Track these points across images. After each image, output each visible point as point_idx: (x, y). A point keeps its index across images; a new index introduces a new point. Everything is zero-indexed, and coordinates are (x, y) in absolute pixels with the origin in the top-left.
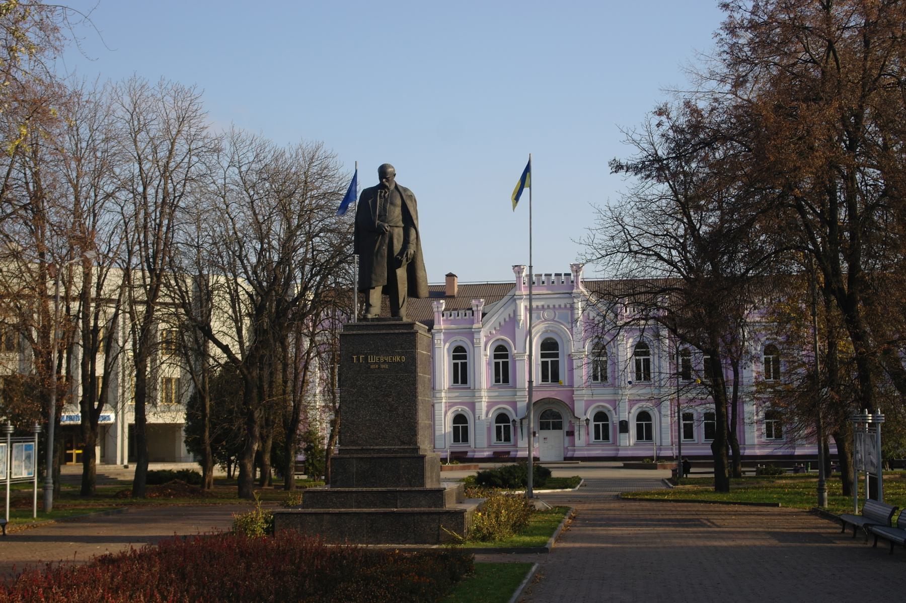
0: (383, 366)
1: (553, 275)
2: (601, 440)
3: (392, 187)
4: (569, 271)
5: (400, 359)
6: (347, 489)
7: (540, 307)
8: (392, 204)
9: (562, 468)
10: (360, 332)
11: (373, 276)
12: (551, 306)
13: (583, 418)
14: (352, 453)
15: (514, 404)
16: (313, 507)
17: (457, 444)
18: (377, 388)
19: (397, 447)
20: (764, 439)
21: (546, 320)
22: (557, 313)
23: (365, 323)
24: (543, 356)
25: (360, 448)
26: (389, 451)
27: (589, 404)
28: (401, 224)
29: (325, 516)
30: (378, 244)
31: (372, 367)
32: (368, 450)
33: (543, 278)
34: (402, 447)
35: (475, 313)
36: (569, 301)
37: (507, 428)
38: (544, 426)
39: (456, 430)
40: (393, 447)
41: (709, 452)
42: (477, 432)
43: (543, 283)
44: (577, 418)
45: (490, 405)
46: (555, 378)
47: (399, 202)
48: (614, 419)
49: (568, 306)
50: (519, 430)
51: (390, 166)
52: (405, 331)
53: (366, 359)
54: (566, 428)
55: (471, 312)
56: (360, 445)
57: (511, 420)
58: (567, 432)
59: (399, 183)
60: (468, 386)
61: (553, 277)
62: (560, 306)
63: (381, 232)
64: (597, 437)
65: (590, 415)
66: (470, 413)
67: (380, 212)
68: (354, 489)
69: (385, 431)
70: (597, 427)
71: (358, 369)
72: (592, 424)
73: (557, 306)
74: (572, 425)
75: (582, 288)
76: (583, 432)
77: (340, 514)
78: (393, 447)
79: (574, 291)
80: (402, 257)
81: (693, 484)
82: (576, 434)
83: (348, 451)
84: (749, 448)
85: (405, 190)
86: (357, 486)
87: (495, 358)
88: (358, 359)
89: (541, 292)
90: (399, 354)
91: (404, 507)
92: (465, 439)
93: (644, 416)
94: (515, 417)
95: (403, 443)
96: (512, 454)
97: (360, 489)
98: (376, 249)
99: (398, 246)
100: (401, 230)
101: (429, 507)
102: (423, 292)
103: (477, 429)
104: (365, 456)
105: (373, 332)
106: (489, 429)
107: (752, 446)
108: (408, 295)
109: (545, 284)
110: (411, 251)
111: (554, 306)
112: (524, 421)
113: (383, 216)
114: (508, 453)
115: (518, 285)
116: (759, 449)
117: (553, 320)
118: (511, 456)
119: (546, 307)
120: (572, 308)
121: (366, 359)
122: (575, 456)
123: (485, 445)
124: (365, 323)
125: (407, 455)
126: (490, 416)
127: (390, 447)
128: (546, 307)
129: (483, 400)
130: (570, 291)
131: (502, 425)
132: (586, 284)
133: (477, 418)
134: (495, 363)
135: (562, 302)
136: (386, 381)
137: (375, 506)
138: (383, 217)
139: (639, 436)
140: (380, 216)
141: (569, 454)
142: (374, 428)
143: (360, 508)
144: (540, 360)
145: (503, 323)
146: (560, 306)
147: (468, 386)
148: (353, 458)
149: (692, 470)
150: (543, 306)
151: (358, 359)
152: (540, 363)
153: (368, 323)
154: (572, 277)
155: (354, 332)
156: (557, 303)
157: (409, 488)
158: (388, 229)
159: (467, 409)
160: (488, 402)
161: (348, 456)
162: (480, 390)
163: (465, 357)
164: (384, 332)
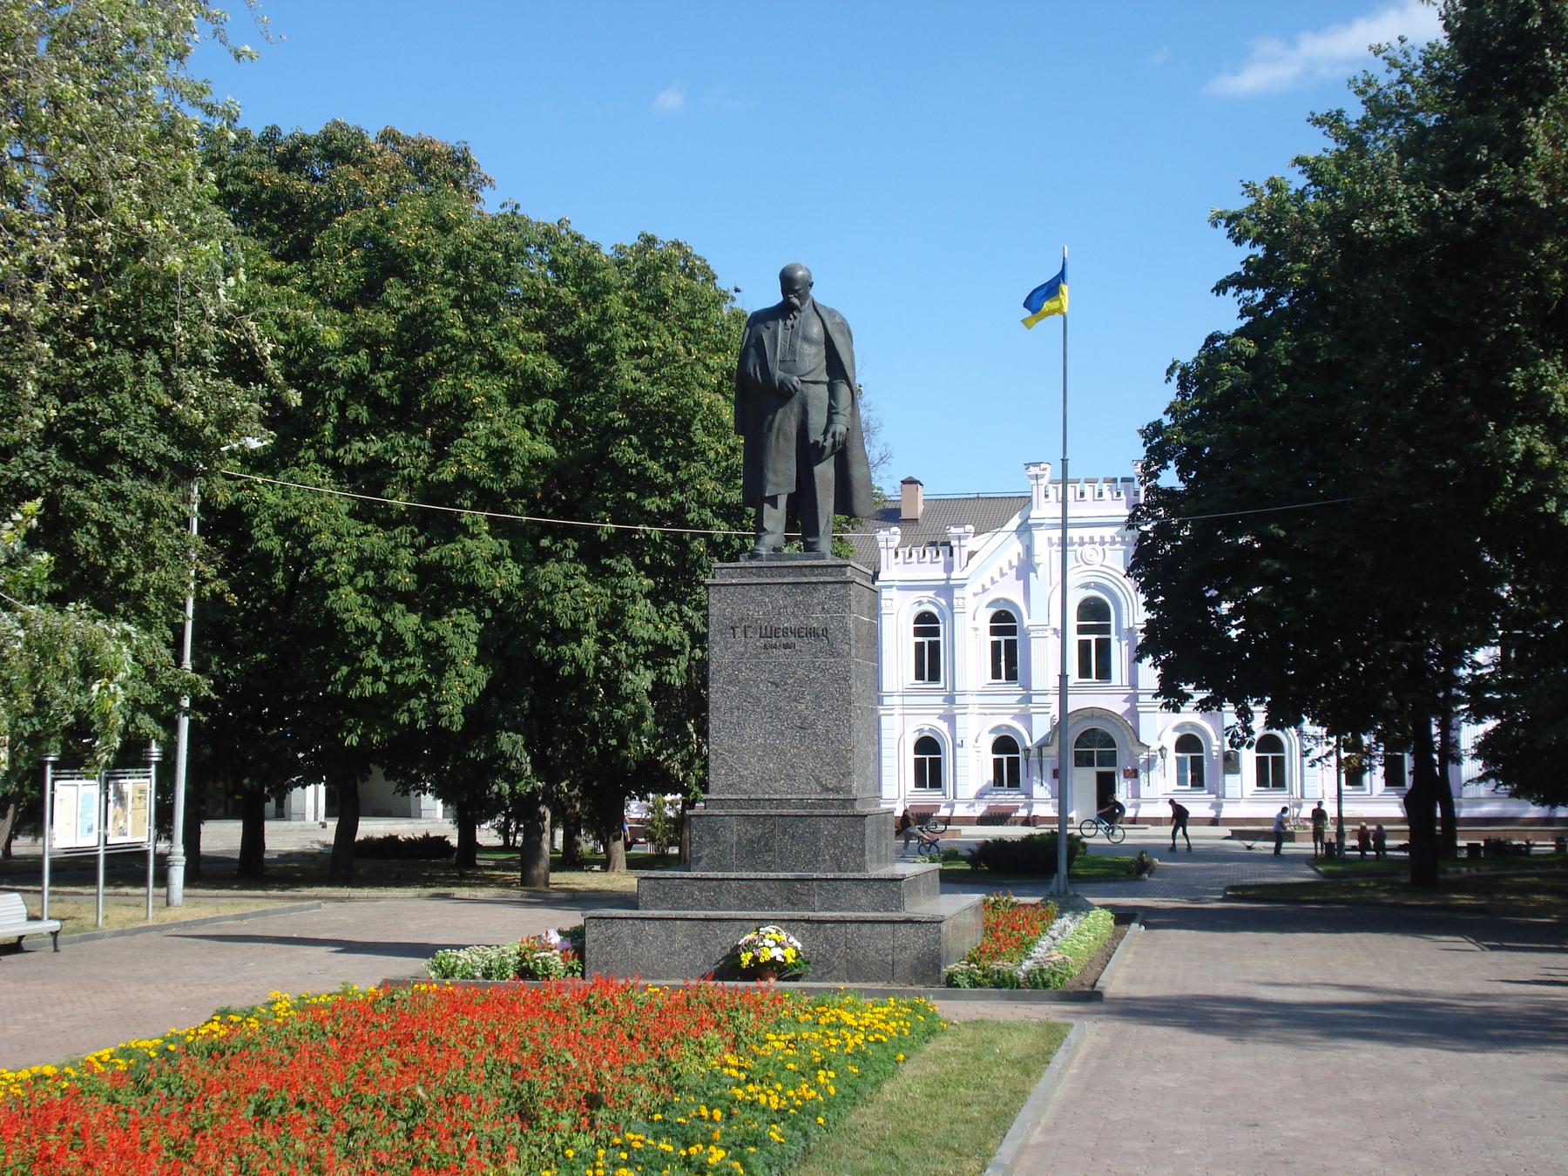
6: (720, 875)
12: (1097, 539)
13: (1155, 746)
14: (729, 807)
16: (656, 907)
22: (1107, 552)
23: (754, 563)
24: (1082, 630)
28: (826, 379)
29: (678, 922)
37: (1013, 764)
39: (919, 764)
46: (1104, 673)
52: (831, 579)
55: (948, 548)
59: (818, 300)
63: (784, 394)
65: (1170, 740)
67: (784, 355)
68: (733, 875)
69: (792, 767)
72: (1172, 755)
74: (1135, 757)
85: (832, 312)
86: (739, 869)
91: (826, 910)
92: (936, 782)
94: (1029, 744)
95: (828, 790)
97: (744, 875)
99: (817, 420)
101: (874, 910)
110: (840, 427)
112: (1045, 751)
113: (789, 364)
125: (833, 812)
131: (1005, 757)
137: (772, 905)
139: (1262, 781)
142: (771, 760)
143: (745, 909)
157: (838, 875)
158: (799, 386)
163: (936, 632)
164: (791, 580)
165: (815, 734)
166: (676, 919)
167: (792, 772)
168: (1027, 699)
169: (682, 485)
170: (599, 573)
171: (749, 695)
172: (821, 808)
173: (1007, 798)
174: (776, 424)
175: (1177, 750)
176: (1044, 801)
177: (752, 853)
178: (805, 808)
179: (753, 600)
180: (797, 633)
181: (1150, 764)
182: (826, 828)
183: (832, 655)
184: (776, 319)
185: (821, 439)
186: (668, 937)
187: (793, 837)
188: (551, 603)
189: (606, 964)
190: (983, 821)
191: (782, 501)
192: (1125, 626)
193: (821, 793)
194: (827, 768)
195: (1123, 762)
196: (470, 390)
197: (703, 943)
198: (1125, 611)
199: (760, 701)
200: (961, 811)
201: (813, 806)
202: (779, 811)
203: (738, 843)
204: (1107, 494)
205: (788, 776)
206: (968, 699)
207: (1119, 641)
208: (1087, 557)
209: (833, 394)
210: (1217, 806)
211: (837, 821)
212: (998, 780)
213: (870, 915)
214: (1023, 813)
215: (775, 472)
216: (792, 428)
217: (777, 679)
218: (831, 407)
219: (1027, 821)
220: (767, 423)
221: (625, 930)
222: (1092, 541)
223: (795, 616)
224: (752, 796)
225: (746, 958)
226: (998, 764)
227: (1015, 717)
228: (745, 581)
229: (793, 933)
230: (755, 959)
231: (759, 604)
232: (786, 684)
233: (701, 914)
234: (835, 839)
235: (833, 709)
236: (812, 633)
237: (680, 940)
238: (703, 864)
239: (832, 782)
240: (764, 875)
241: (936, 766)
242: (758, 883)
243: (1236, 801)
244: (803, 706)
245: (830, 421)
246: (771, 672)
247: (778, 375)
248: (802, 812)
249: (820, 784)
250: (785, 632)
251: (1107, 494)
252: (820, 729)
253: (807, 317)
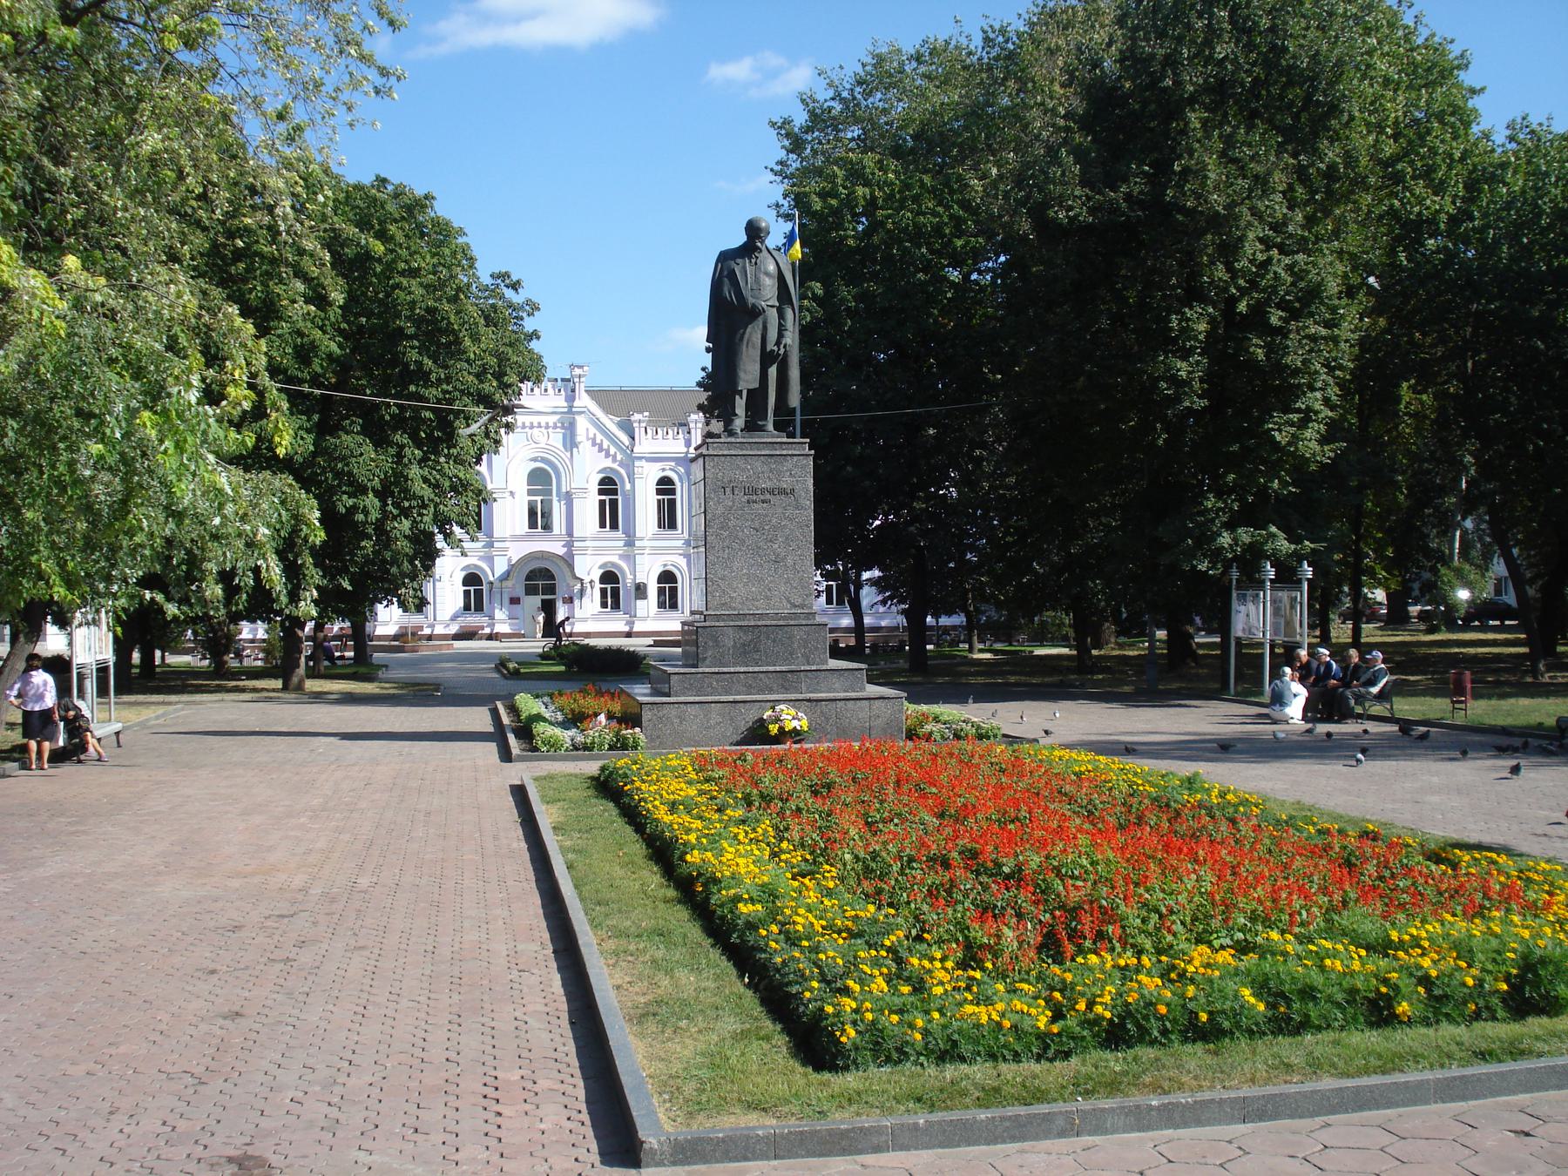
3: (764, 248)
6: (732, 670)
12: (543, 424)
13: (587, 580)
16: (684, 694)
24: (530, 493)
35: (693, 431)
37: (479, 594)
41: (902, 620)
46: (547, 527)
48: (627, 581)
55: (686, 428)
63: (755, 313)
64: (604, 605)
65: (596, 575)
70: (603, 592)
72: (598, 586)
74: (571, 588)
83: (718, 617)
93: (667, 577)
94: (491, 579)
97: (751, 669)
99: (773, 335)
137: (771, 691)
138: (756, 292)
139: (661, 605)
164: (767, 452)
168: (490, 545)
169: (448, 380)
170: (380, 442)
171: (736, 537)
173: (473, 620)
174: (746, 336)
175: (602, 582)
176: (503, 622)
177: (745, 653)
179: (738, 467)
180: (771, 492)
181: (582, 592)
182: (798, 634)
183: (797, 508)
184: (743, 257)
185: (776, 348)
186: (705, 716)
187: (774, 641)
188: (347, 465)
189: (658, 737)
190: (458, 637)
191: (745, 394)
192: (564, 490)
195: (561, 591)
196: (279, 295)
197: (731, 719)
198: (563, 479)
200: (439, 630)
201: (784, 618)
202: (764, 623)
203: (734, 646)
204: (550, 391)
205: (767, 597)
206: (646, 543)
207: (559, 501)
208: (536, 438)
209: (781, 316)
210: (630, 623)
211: (806, 628)
212: (467, 608)
213: (842, 695)
214: (487, 631)
216: (757, 339)
217: (757, 525)
218: (780, 325)
219: (490, 637)
220: (738, 336)
221: (673, 712)
222: (539, 426)
223: (770, 479)
225: (774, 729)
226: (467, 593)
227: (481, 558)
228: (745, 452)
229: (798, 709)
230: (781, 729)
231: (743, 470)
233: (731, 698)
234: (806, 641)
236: (783, 492)
237: (715, 718)
238: (707, 662)
239: (799, 601)
240: (764, 669)
242: (761, 675)
243: (644, 619)
245: (781, 335)
247: (751, 301)
248: (781, 623)
249: (789, 602)
250: (763, 491)
251: (550, 391)
252: (790, 561)
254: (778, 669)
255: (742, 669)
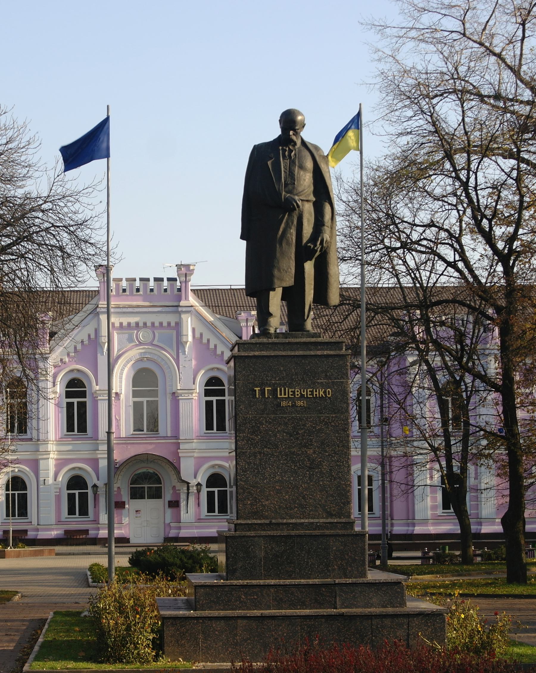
0: (300, 403)
1: (124, 280)
2: (217, 513)
3: (299, 143)
4: (175, 275)
5: (325, 392)
6: (262, 582)
7: (133, 325)
8: (302, 167)
9: (70, 554)
10: (264, 353)
11: (276, 272)
13: (193, 482)
14: (255, 530)
15: (94, 463)
16: (210, 609)
17: (11, 519)
18: (291, 436)
19: (322, 520)
20: (440, 511)
21: (141, 344)
22: (157, 335)
23: (265, 340)
24: (135, 394)
25: (267, 521)
26: (311, 526)
27: (200, 461)
29: (239, 621)
30: (283, 226)
31: (284, 404)
32: (278, 524)
33: (138, 283)
34: (329, 520)
36: (172, 319)
37: (84, 497)
38: (136, 494)
40: (316, 520)
42: (41, 502)
43: (124, 291)
44: (184, 481)
45: (60, 464)
47: (309, 164)
49: (173, 324)
50: (192, 499)
51: (300, 113)
52: (332, 353)
53: (274, 392)
54: (168, 496)
56: (266, 518)
57: (90, 486)
58: (169, 502)
59: (306, 139)
60: (28, 436)
61: (152, 283)
62: (161, 324)
64: (211, 509)
65: (202, 478)
66: (32, 475)
69: (304, 498)
70: (210, 495)
71: (262, 407)
72: (205, 491)
73: (157, 324)
75: (192, 300)
76: (192, 500)
77: (263, 618)
78: (316, 520)
79: (182, 303)
80: (315, 245)
81: (432, 573)
82: (183, 504)
83: (250, 527)
84: (420, 524)
85: (317, 148)
86: (267, 577)
87: (67, 397)
88: (262, 392)
89: (135, 303)
90: (322, 385)
91: (346, 607)
92: (23, 512)
94: (95, 481)
95: (330, 515)
96: (92, 533)
97: (282, 582)
98: (280, 232)
99: (308, 230)
100: (311, 205)
101: (383, 607)
102: (334, 298)
103: (41, 497)
104: (279, 533)
105: (284, 353)
106: (58, 498)
107: (425, 522)
108: (313, 303)
109: (141, 292)
111: (153, 324)
114: (86, 532)
115: (102, 293)
116: (434, 524)
117: (152, 344)
118: (89, 536)
119: (141, 324)
120: (178, 325)
121: (274, 392)
122: (181, 535)
123: (53, 520)
124: (265, 340)
126: (60, 479)
127: (312, 521)
128: (141, 324)
129: (52, 456)
130: (175, 304)
131: (77, 492)
132: (199, 293)
133: (41, 482)
134: (68, 403)
135: (166, 319)
136: (304, 425)
137: (304, 606)
138: (290, 187)
140: (286, 185)
141: (173, 533)
142: (287, 492)
144: (131, 400)
145: (79, 347)
146: (169, 324)
147: (28, 436)
148: (259, 537)
149: (395, 554)
150: (137, 324)
151: (262, 392)
152: (131, 404)
153: (270, 341)
154: (178, 283)
155: (257, 353)
156: (157, 319)
159: (27, 469)
160: (56, 460)
161: (253, 533)
162: (46, 442)
164: (301, 353)
165: (321, 472)
166: (238, 617)
167: (303, 502)
172: (328, 529)
178: (315, 529)
193: (327, 518)
194: (331, 498)
199: (277, 447)
215: (279, 270)
224: (273, 521)
232: (297, 433)
233: (257, 613)
235: (335, 453)
240: (297, 581)
241: (23, 499)
244: (312, 451)
246: (286, 424)
248: (317, 532)
253: (300, 151)
254: (311, 581)
255: (273, 582)
